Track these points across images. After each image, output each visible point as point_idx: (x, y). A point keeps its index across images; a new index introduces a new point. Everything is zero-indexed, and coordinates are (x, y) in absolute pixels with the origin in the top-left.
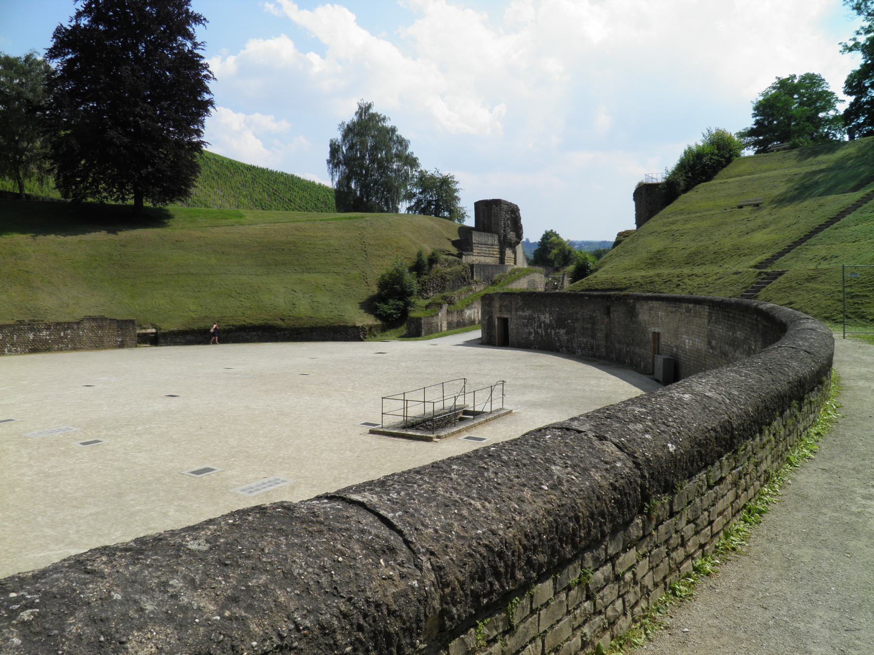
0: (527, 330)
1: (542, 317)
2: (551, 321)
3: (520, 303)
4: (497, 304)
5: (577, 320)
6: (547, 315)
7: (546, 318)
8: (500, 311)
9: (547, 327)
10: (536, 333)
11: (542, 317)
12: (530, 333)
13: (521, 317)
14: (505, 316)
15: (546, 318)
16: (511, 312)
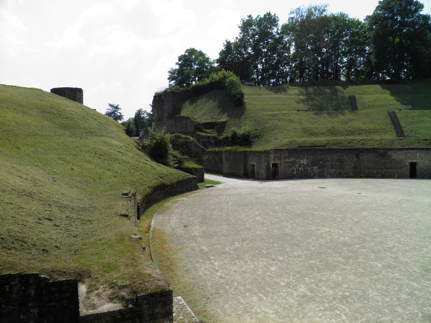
0: (291, 169)
1: (302, 162)
2: (307, 163)
3: (287, 155)
4: (272, 156)
5: (327, 161)
6: (305, 160)
7: (305, 162)
8: (274, 160)
9: (304, 166)
10: (298, 170)
11: (302, 162)
12: (293, 170)
13: (287, 162)
14: (278, 162)
15: (305, 162)
16: (281, 160)
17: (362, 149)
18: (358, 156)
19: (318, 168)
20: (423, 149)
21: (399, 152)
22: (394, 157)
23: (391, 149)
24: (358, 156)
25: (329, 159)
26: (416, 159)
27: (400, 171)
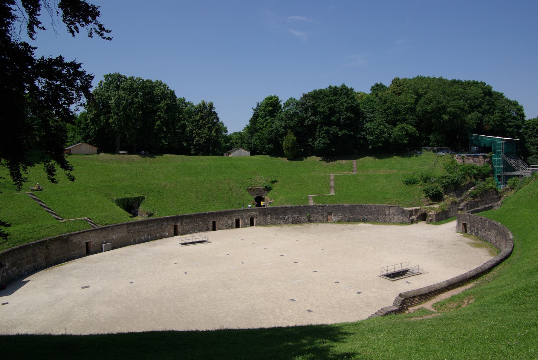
5: (23, 259)
17: (50, 240)
18: (47, 248)
19: (17, 268)
20: (93, 230)
21: (78, 236)
22: (74, 241)
23: (71, 235)
24: (47, 248)
25: (24, 257)
26: (90, 239)
27: (79, 251)
